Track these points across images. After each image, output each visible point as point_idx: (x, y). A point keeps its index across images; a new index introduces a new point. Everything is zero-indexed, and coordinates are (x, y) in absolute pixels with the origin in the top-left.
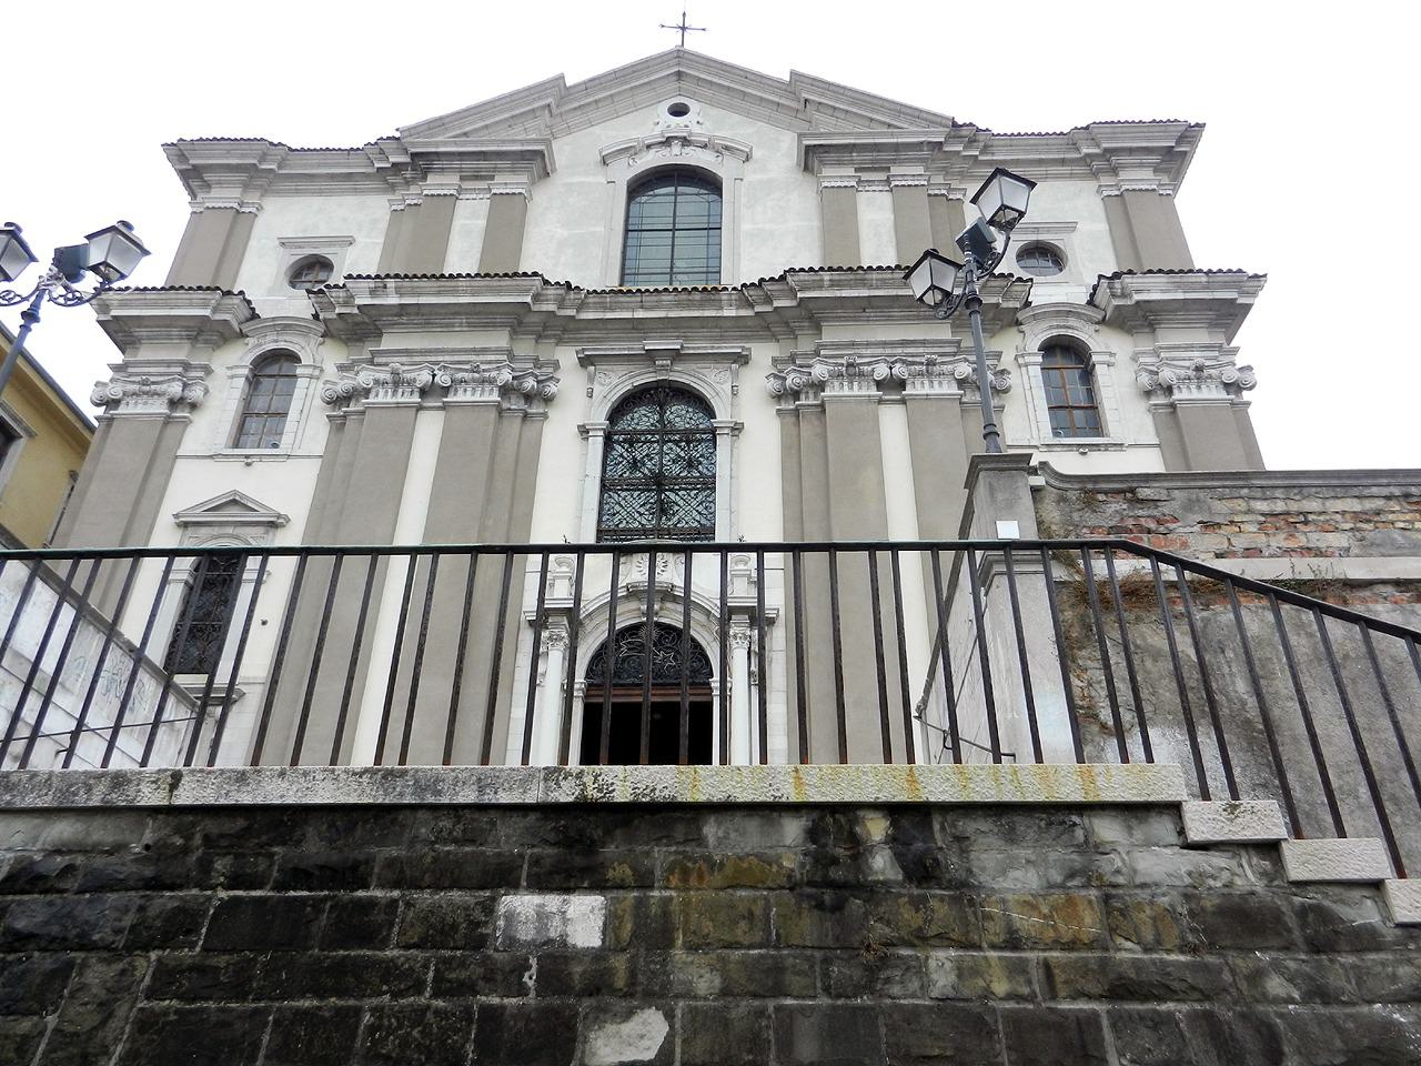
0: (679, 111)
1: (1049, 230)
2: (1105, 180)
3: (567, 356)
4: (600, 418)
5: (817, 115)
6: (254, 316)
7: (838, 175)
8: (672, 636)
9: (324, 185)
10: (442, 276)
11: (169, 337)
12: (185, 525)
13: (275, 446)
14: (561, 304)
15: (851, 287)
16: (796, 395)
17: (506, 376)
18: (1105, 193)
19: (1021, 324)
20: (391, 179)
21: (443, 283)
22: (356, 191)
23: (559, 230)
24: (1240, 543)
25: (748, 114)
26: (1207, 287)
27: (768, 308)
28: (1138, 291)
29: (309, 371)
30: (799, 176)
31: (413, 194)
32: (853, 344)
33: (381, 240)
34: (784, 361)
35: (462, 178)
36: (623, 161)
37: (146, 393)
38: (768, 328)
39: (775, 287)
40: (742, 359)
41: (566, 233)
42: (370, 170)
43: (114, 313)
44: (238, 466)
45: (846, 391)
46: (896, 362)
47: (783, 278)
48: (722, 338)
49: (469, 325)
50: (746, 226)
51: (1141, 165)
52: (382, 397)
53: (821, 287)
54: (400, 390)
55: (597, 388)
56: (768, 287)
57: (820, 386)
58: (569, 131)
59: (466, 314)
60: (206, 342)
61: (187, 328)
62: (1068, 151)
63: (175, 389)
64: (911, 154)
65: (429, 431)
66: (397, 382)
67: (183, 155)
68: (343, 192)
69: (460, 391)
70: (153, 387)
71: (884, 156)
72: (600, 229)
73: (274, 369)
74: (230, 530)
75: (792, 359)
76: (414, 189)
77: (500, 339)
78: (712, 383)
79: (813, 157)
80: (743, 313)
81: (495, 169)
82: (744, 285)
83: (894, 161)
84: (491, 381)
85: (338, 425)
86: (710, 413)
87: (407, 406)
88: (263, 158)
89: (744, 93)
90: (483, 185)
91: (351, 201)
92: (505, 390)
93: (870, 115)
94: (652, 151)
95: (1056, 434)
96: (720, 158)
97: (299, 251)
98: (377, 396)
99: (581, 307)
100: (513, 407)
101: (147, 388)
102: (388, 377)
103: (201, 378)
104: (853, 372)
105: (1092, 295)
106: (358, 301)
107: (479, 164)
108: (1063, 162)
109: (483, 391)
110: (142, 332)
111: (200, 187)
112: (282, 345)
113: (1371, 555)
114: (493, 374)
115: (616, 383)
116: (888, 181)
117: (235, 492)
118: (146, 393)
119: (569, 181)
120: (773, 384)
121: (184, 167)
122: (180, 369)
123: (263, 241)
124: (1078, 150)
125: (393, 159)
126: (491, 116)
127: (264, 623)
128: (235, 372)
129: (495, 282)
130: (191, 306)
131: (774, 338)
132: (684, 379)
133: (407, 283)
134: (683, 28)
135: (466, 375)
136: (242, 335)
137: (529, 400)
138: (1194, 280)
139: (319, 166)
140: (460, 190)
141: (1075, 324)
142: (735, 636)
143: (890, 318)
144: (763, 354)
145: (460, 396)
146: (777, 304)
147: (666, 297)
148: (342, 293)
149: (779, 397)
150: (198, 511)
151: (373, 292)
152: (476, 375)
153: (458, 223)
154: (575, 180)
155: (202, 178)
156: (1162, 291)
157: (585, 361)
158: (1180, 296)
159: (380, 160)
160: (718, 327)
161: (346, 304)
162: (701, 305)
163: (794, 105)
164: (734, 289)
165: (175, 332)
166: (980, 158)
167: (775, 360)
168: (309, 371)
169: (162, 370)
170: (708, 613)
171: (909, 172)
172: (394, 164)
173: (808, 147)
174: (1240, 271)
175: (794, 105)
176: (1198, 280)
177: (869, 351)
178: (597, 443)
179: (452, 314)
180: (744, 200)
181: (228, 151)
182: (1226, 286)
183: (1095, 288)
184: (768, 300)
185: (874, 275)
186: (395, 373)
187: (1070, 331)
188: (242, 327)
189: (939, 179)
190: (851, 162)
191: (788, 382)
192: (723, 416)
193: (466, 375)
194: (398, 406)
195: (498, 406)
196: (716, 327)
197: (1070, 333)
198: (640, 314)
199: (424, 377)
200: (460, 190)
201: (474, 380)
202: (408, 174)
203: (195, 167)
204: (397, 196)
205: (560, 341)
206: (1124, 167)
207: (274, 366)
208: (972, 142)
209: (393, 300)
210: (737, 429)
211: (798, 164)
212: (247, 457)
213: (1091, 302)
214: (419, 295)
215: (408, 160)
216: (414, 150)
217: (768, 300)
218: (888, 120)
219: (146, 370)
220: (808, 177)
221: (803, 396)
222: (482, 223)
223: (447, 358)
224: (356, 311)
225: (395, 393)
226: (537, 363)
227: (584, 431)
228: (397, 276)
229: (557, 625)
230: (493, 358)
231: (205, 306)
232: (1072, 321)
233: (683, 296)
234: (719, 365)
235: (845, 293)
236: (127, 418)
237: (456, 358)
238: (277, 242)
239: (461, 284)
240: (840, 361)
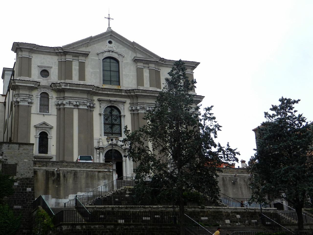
0: (110, 42)
3: (96, 98)
4: (102, 113)
5: (137, 51)
6: (39, 85)
7: (140, 65)
8: (117, 151)
9: (44, 53)
11: (25, 88)
12: (36, 127)
13: (48, 113)
14: (96, 90)
15: (144, 93)
16: (134, 111)
17: (88, 104)
21: (78, 85)
22: (50, 55)
23: (91, 69)
25: (123, 45)
27: (130, 94)
29: (51, 98)
30: (133, 62)
31: (63, 58)
32: (143, 103)
33: (57, 67)
34: (131, 103)
35: (73, 56)
36: (101, 54)
37: (24, 101)
38: (129, 96)
39: (132, 91)
40: (125, 102)
41: (92, 70)
42: (54, 52)
43: (16, 84)
44: (42, 116)
45: (142, 112)
46: (150, 107)
47: (133, 90)
48: (121, 97)
49: (80, 92)
50: (124, 73)
51: (189, 68)
52: (67, 106)
53: (139, 92)
55: (102, 106)
56: (131, 91)
57: (138, 110)
58: (90, 45)
60: (31, 90)
61: (29, 87)
63: (30, 101)
64: (153, 62)
65: (76, 113)
66: (70, 103)
67: (18, 45)
68: (48, 55)
69: (80, 106)
70: (25, 100)
71: (148, 62)
72: (98, 70)
73: (43, 95)
74: (44, 129)
75: (133, 103)
76: (63, 57)
77: (85, 96)
78: (120, 107)
79: (136, 61)
81: (79, 56)
84: (86, 104)
85: (59, 110)
86: (120, 112)
87: (72, 108)
88: (34, 47)
89: (123, 42)
90: (77, 58)
91: (49, 57)
92: (87, 107)
93: (146, 53)
94: (107, 52)
96: (119, 56)
97: (42, 68)
98: (66, 105)
99: (99, 90)
101: (24, 100)
102: (68, 102)
103: (32, 97)
104: (143, 108)
106: (62, 87)
107: (77, 55)
109: (84, 106)
110: (21, 87)
112: (45, 91)
114: (86, 103)
115: (104, 105)
116: (149, 67)
117: (44, 122)
118: (24, 101)
119: (92, 58)
120: (130, 108)
121: (17, 47)
122: (29, 96)
123: (34, 65)
126: (78, 44)
127: (53, 145)
128: (38, 97)
129: (86, 86)
130: (31, 84)
131: (130, 98)
132: (116, 106)
133: (71, 85)
134: (109, 18)
135: (82, 103)
136: (37, 88)
137: (91, 108)
139: (44, 49)
140: (73, 59)
143: (149, 98)
144: (128, 101)
145: (81, 107)
146: (132, 94)
147: (113, 90)
148: (59, 85)
149: (131, 111)
150: (38, 125)
151: (65, 86)
152: (83, 103)
153: (73, 67)
154: (92, 58)
155: (21, 50)
157: (99, 100)
160: (121, 96)
161: (59, 86)
162: (119, 92)
163: (132, 46)
165: (26, 88)
166: (164, 63)
167: (130, 103)
168: (51, 98)
169: (25, 96)
171: (152, 66)
174: (201, 96)
175: (132, 46)
177: (146, 104)
178: (102, 117)
180: (123, 67)
181: (28, 45)
182: (199, 98)
184: (130, 93)
185: (148, 91)
186: (70, 102)
189: (157, 67)
190: (142, 62)
191: (133, 108)
192: (122, 114)
193: (82, 103)
194: (70, 108)
195: (87, 109)
198: (109, 93)
199: (75, 103)
200: (73, 59)
201: (83, 104)
202: (62, 54)
204: (60, 57)
205: (94, 95)
207: (45, 97)
208: (163, 61)
209: (68, 87)
210: (124, 116)
211: (133, 60)
212: (44, 114)
214: (73, 87)
215: (63, 52)
216: (65, 51)
217: (130, 93)
218: (149, 55)
219: (23, 95)
220: (134, 63)
222: (78, 68)
223: (77, 99)
224: (61, 88)
225: (69, 105)
226: (92, 100)
227: (100, 114)
228: (70, 83)
229: (101, 150)
230: (85, 99)
231: (33, 84)
233: (116, 90)
234: (121, 103)
235: (143, 94)
236: (21, 105)
237: (79, 99)
238: (37, 66)
240: (141, 106)
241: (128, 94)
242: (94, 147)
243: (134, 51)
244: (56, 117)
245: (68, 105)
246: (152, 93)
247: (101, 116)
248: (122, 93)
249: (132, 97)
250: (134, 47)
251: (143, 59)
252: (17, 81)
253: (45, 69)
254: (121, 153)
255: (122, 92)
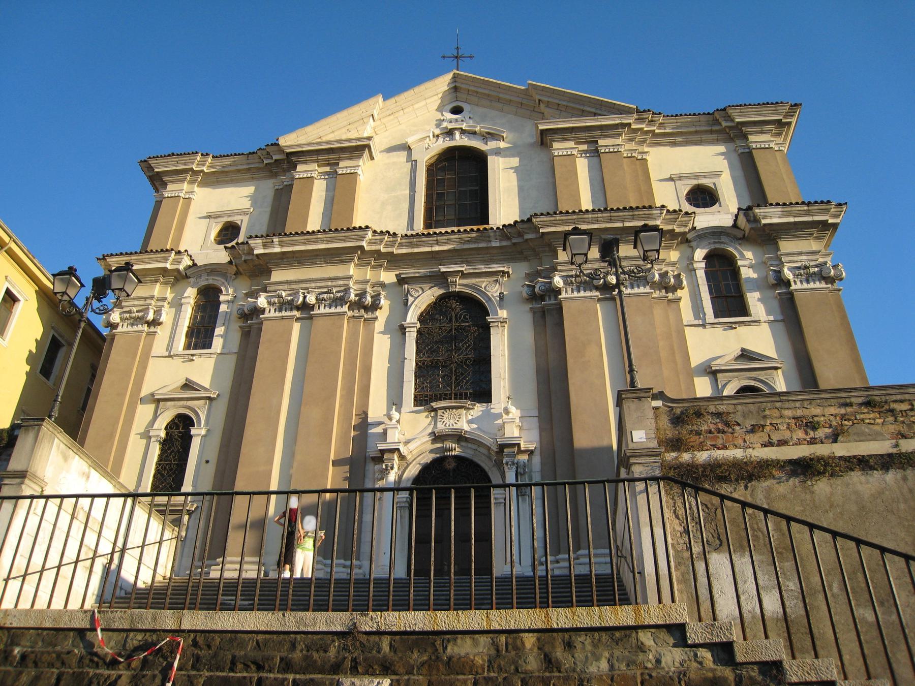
1: (705, 177)
2: (739, 143)
10: (308, 232)
18: (740, 151)
19: (690, 242)
20: (275, 170)
24: (775, 438)
26: (808, 213)
28: (765, 217)
33: (269, 209)
38: (521, 253)
39: (525, 226)
54: (284, 308)
59: (323, 255)
62: (714, 124)
80: (504, 243)
81: (340, 159)
82: (504, 226)
83: (601, 137)
95: (716, 316)
100: (355, 315)
105: (735, 221)
108: (711, 132)
111: (160, 185)
112: (211, 282)
113: (850, 441)
120: (525, 292)
124: (720, 124)
125: (275, 157)
127: (207, 462)
131: (526, 259)
134: (457, 57)
138: (799, 209)
141: (723, 240)
142: (507, 463)
146: (527, 237)
148: (246, 247)
156: (780, 217)
158: (792, 220)
159: (267, 158)
164: (498, 228)
170: (489, 449)
172: (276, 160)
173: (542, 131)
176: (802, 209)
179: (314, 256)
183: (737, 216)
184: (520, 235)
187: (722, 245)
188: (187, 272)
194: (283, 318)
196: (487, 254)
197: (722, 246)
198: (437, 248)
201: (330, 299)
203: (158, 173)
206: (751, 133)
209: (277, 250)
213: (735, 225)
216: (288, 151)
217: (520, 235)
221: (547, 298)
232: (724, 238)
239: (319, 236)
240: (570, 274)
241: (514, 241)
242: (367, 454)
243: (542, 115)
244: (234, 357)
245: (275, 312)
246: (611, 220)
247: (404, 334)
248: (490, 241)
249: (534, 250)
250: (537, 101)
251: (571, 125)
252: (114, 259)
253: (229, 219)
254: (487, 469)
255: (489, 236)
